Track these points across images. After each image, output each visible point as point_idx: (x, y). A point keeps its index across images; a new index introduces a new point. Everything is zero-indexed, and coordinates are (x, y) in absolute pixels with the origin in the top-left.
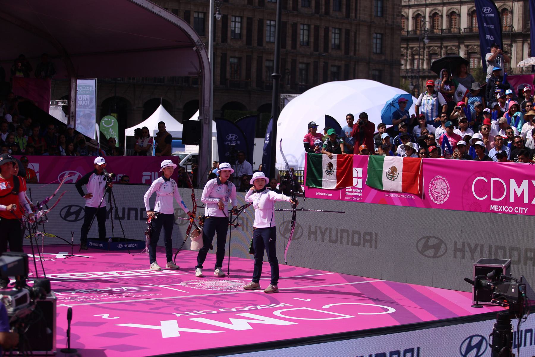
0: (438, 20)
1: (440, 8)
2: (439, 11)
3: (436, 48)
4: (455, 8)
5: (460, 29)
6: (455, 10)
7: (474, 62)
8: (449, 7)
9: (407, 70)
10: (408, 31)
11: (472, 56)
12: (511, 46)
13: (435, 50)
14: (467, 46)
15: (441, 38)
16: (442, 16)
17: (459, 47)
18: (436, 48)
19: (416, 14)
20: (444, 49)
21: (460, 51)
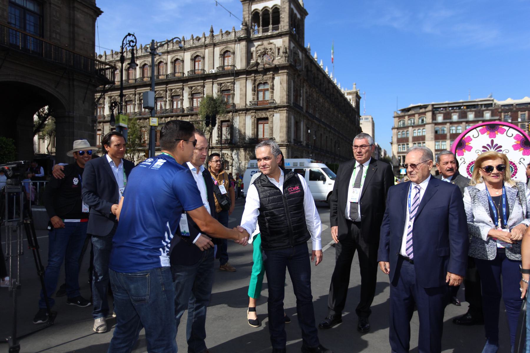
0: (163, 67)
1: (165, 57)
2: (164, 59)
3: (162, 92)
4: (179, 55)
5: (183, 73)
6: (178, 57)
7: (197, 102)
8: (173, 55)
9: (135, 113)
10: (136, 80)
11: (196, 96)
12: (234, 83)
13: (161, 94)
14: (191, 88)
15: (167, 82)
16: (166, 64)
17: (183, 89)
18: (162, 92)
19: (143, 64)
20: (168, 92)
21: (184, 92)
